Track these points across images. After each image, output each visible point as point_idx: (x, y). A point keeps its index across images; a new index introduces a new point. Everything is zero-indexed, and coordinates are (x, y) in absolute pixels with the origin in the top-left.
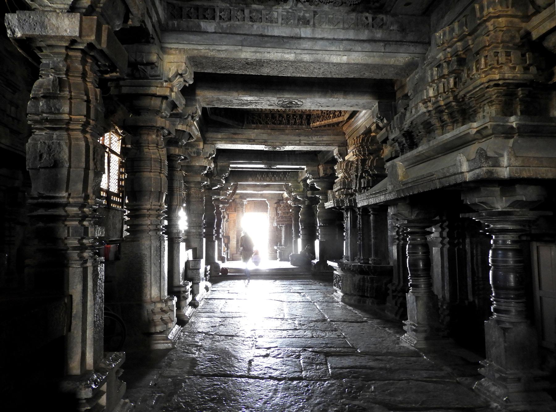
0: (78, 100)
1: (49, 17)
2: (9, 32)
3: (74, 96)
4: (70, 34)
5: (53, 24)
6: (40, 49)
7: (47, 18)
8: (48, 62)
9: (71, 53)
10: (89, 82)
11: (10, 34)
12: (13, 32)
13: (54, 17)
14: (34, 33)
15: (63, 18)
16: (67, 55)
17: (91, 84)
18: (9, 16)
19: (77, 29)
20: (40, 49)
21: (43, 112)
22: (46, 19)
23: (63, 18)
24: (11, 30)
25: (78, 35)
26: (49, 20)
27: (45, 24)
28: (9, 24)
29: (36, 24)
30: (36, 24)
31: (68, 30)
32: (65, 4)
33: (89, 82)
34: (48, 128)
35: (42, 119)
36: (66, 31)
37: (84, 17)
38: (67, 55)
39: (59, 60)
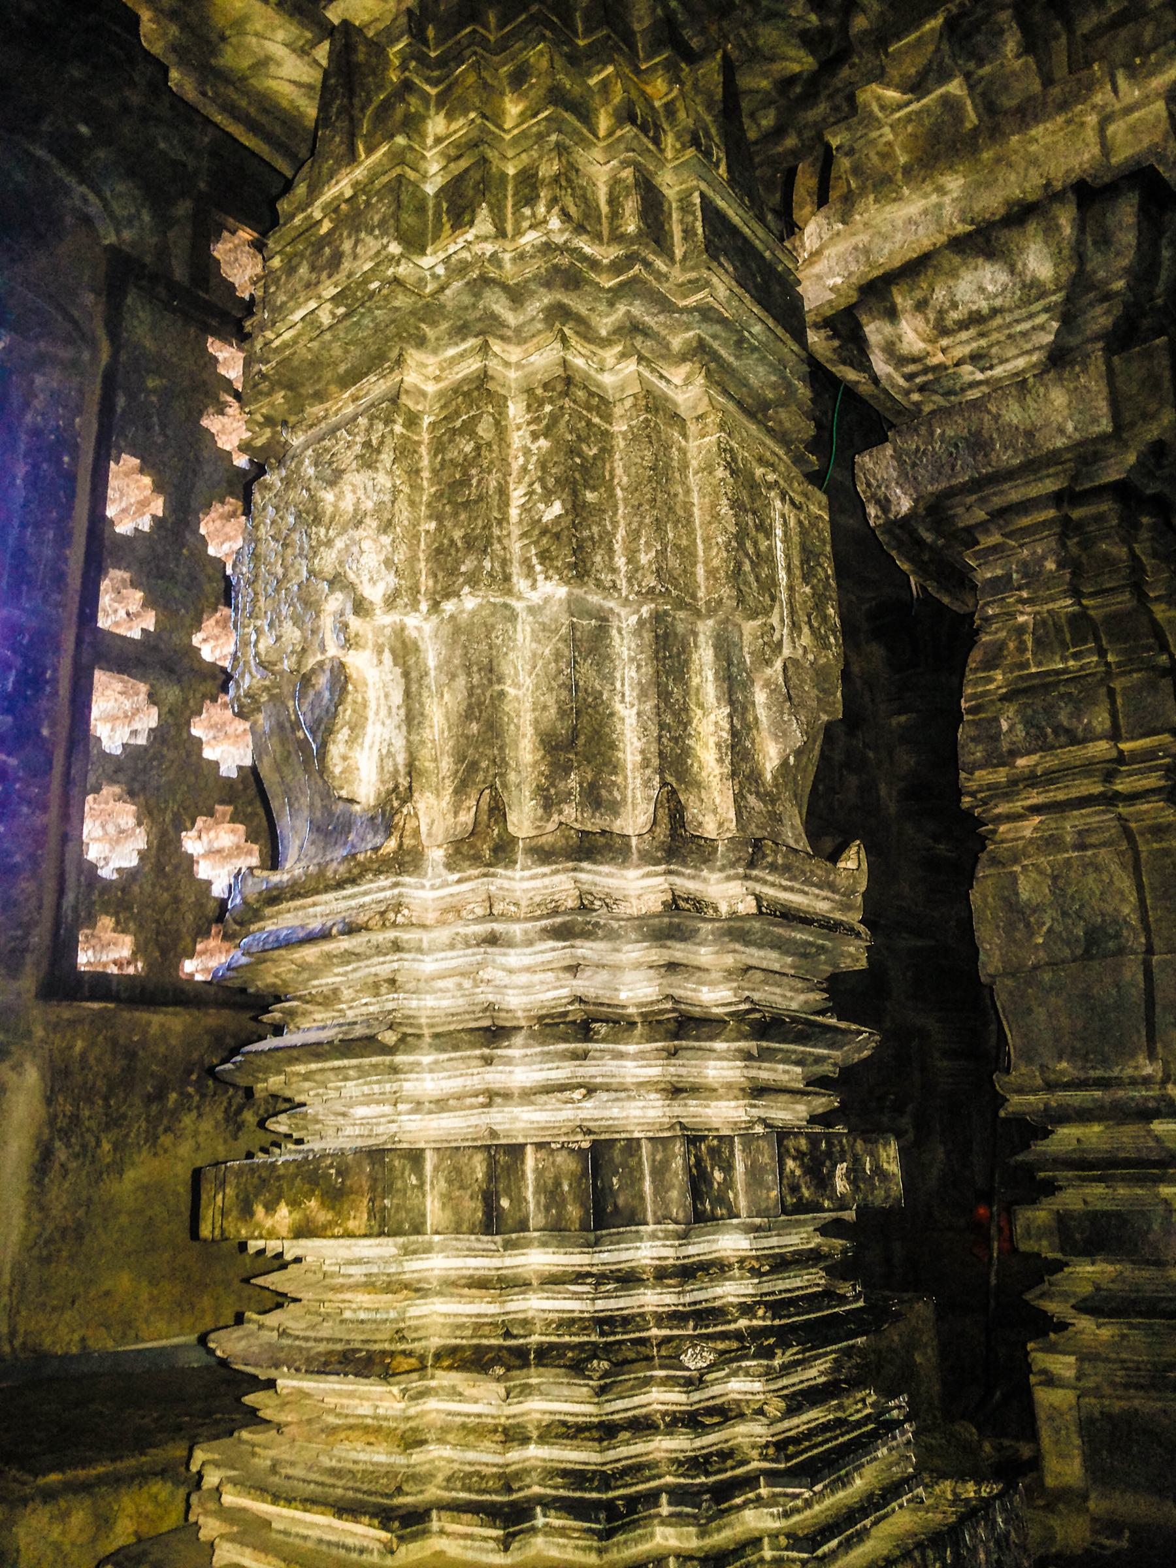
0: (1135, 675)
1: (994, 410)
2: (872, 510)
3: (1119, 665)
4: (1077, 436)
5: (1010, 425)
6: (969, 537)
7: (989, 412)
8: (999, 572)
9: (1077, 514)
10: (1158, 599)
11: (877, 517)
12: (884, 505)
13: (1011, 401)
14: (954, 482)
15: (1042, 390)
16: (1066, 521)
17: (1163, 606)
18: (867, 459)
19: (1103, 406)
20: (969, 537)
21: (1014, 753)
22: (987, 417)
23: (1042, 390)
24: (878, 502)
25: (1110, 430)
26: (997, 417)
27: (986, 436)
28: (869, 485)
29: (956, 446)
30: (956, 446)
31: (1070, 427)
32: (1028, 352)
33: (1158, 599)
34: (1036, 810)
35: (1013, 782)
36: (1061, 431)
37: (1116, 359)
38: (1066, 521)
39: (1039, 551)
